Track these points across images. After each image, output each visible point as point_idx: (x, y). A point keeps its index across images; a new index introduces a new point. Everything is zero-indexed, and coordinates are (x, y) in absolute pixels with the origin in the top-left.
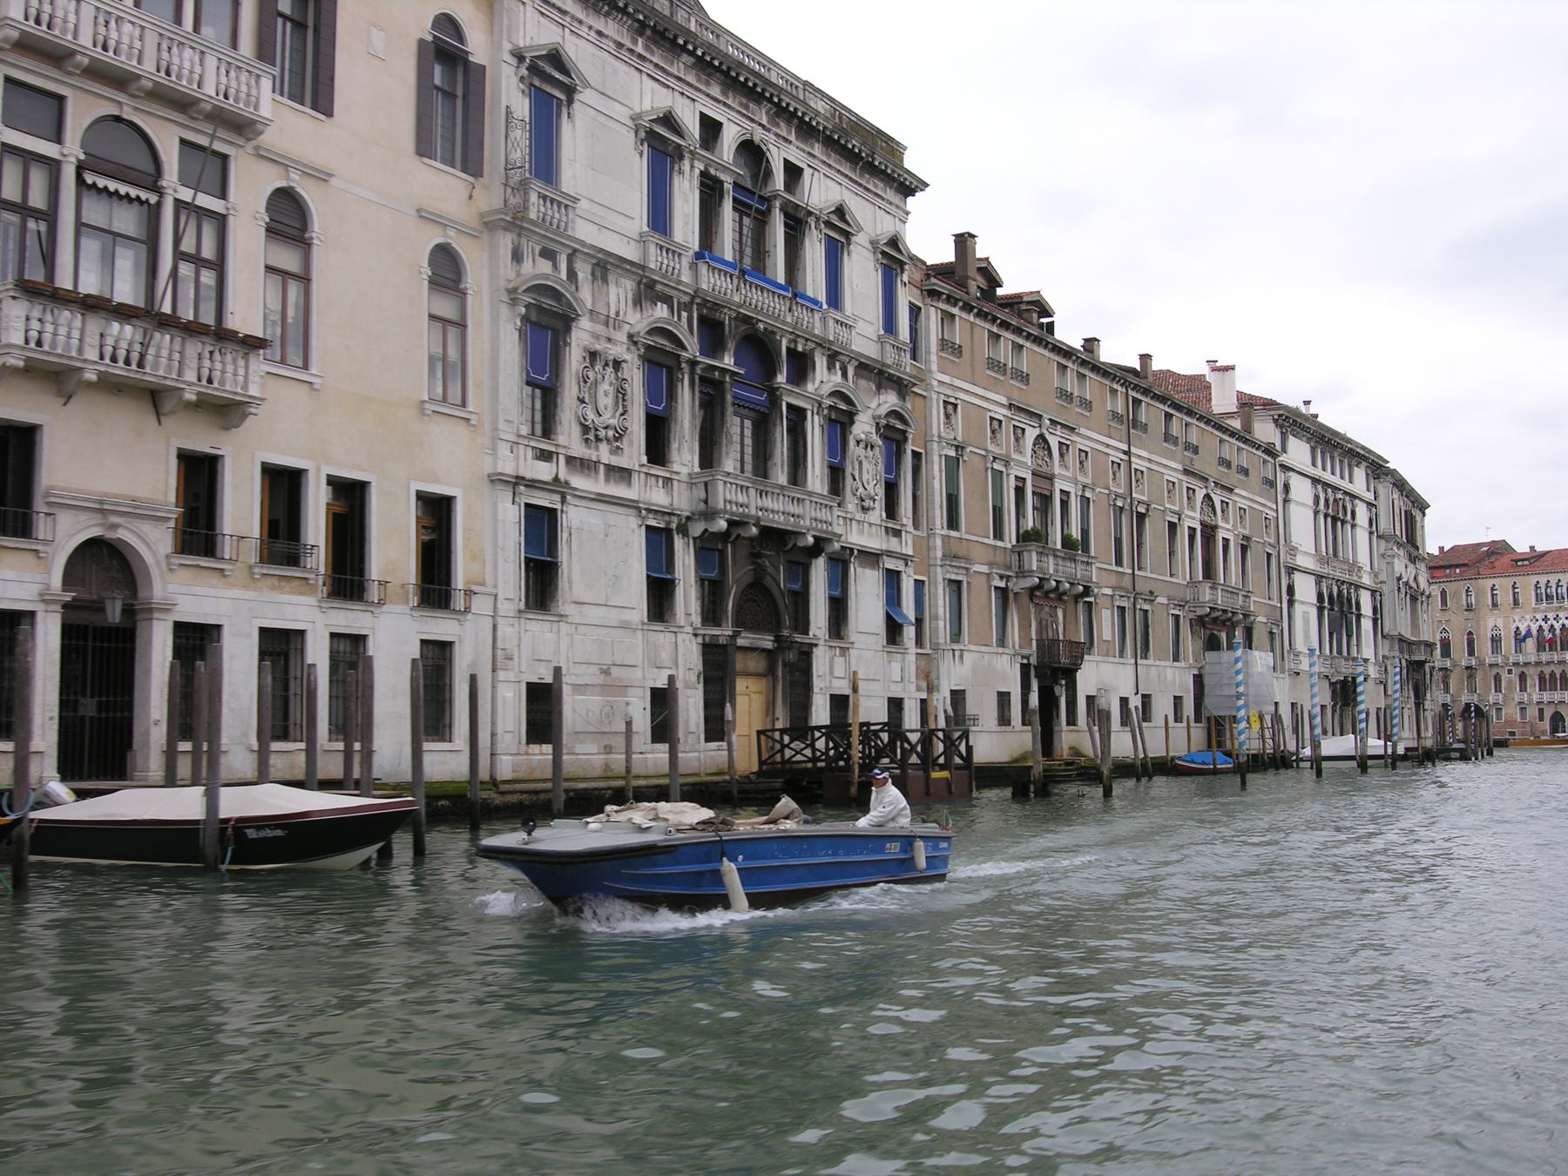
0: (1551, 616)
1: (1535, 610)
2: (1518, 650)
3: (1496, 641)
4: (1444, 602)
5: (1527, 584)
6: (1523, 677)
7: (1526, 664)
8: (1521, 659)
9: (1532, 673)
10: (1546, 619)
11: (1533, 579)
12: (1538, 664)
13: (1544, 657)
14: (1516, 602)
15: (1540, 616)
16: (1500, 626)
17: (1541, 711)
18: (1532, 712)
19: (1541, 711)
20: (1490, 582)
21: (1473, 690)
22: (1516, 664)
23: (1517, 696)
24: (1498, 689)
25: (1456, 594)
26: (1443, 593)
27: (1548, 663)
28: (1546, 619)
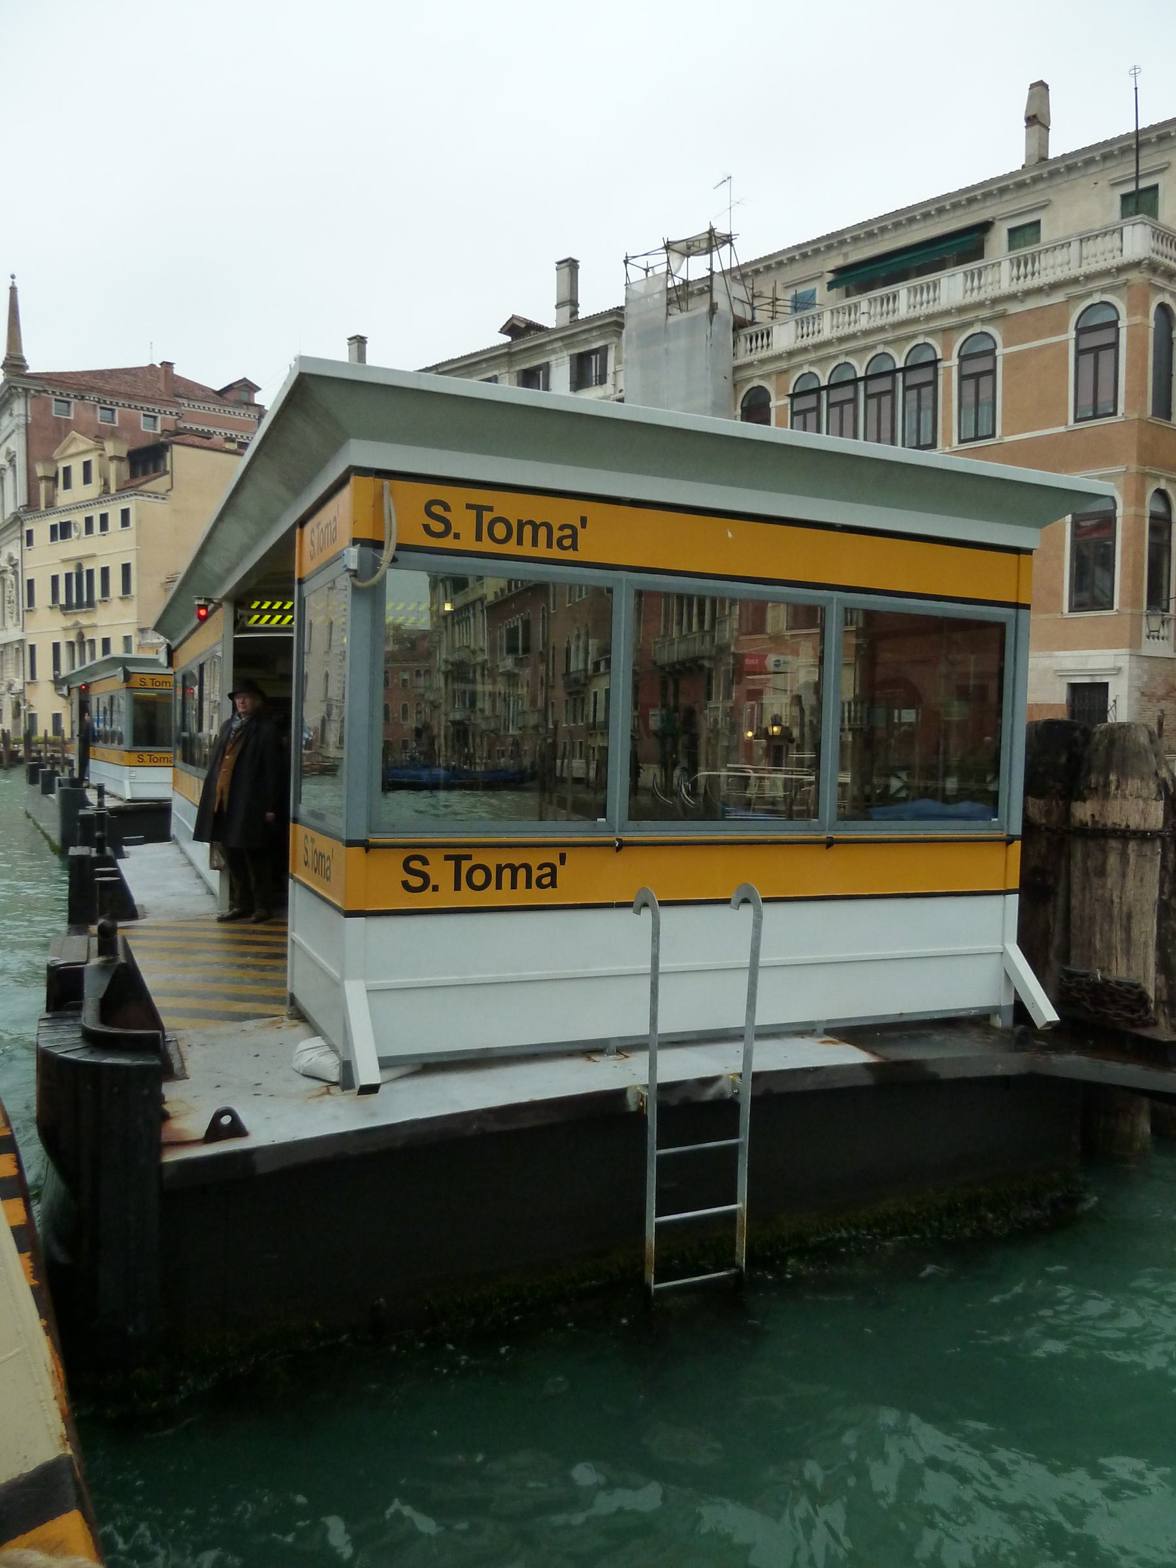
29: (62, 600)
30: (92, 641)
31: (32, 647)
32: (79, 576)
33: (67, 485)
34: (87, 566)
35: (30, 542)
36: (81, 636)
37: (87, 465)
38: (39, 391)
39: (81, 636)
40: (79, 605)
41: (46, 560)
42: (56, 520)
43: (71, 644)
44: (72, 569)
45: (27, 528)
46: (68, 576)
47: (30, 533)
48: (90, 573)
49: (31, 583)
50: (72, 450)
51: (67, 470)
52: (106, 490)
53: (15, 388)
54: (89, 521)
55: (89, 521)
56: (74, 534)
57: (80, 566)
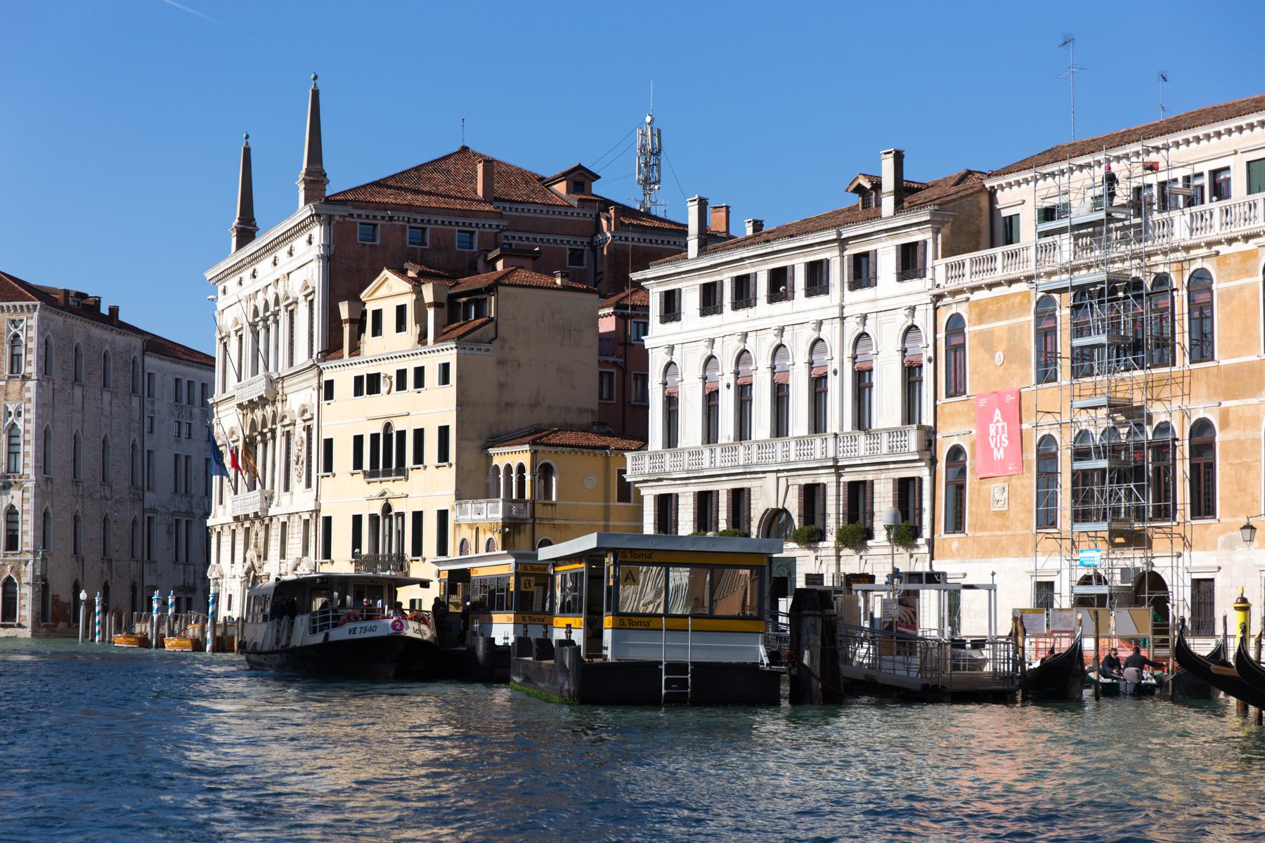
29: (366, 465)
30: (402, 515)
31: (328, 521)
32: (388, 437)
33: (377, 331)
34: (397, 426)
35: (329, 394)
36: (387, 508)
37: (401, 310)
38: (344, 216)
39: (387, 508)
40: (387, 473)
41: (350, 419)
42: (364, 370)
43: (374, 519)
44: (378, 428)
45: (327, 376)
46: (375, 437)
47: (329, 386)
48: (402, 435)
49: (329, 443)
50: (383, 291)
51: (377, 314)
52: (422, 338)
54: (402, 374)
55: (402, 374)
56: (384, 388)
57: (388, 426)
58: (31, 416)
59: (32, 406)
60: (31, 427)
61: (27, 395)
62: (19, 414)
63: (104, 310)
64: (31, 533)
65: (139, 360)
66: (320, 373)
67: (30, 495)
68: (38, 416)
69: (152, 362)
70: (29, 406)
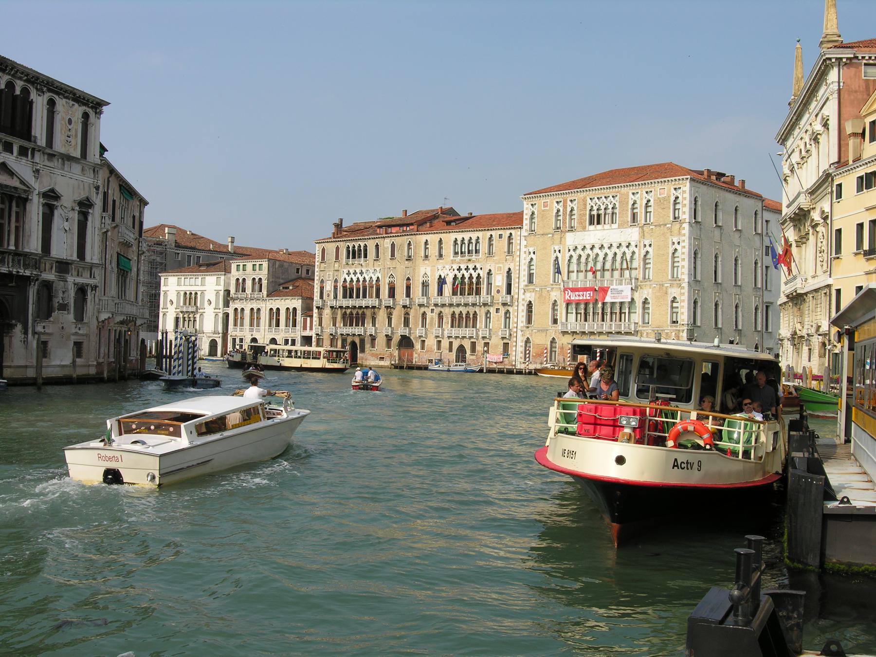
0: (463, 267)
1: (453, 262)
2: (440, 292)
3: (425, 285)
4: (393, 255)
5: (449, 238)
6: (440, 316)
7: (443, 305)
8: (439, 300)
9: (447, 311)
10: (459, 269)
11: (453, 236)
12: (451, 305)
13: (455, 300)
14: (441, 256)
15: (456, 267)
16: (429, 274)
17: (451, 343)
18: (445, 343)
19: (451, 343)
20: (422, 238)
21: (406, 323)
22: (436, 305)
23: (435, 330)
24: (424, 325)
25: (401, 245)
26: (393, 245)
27: (458, 305)
28: (459, 269)
29: (866, 246)
31: (838, 291)
35: (839, 195)
45: (836, 183)
49: (839, 231)
53: (830, 59)
58: (686, 244)
59: (686, 238)
60: (686, 250)
61: (683, 232)
62: (679, 243)
63: (736, 183)
64: (686, 314)
65: (759, 213)
66: (833, 180)
67: (686, 290)
68: (690, 244)
69: (767, 215)
70: (683, 238)
